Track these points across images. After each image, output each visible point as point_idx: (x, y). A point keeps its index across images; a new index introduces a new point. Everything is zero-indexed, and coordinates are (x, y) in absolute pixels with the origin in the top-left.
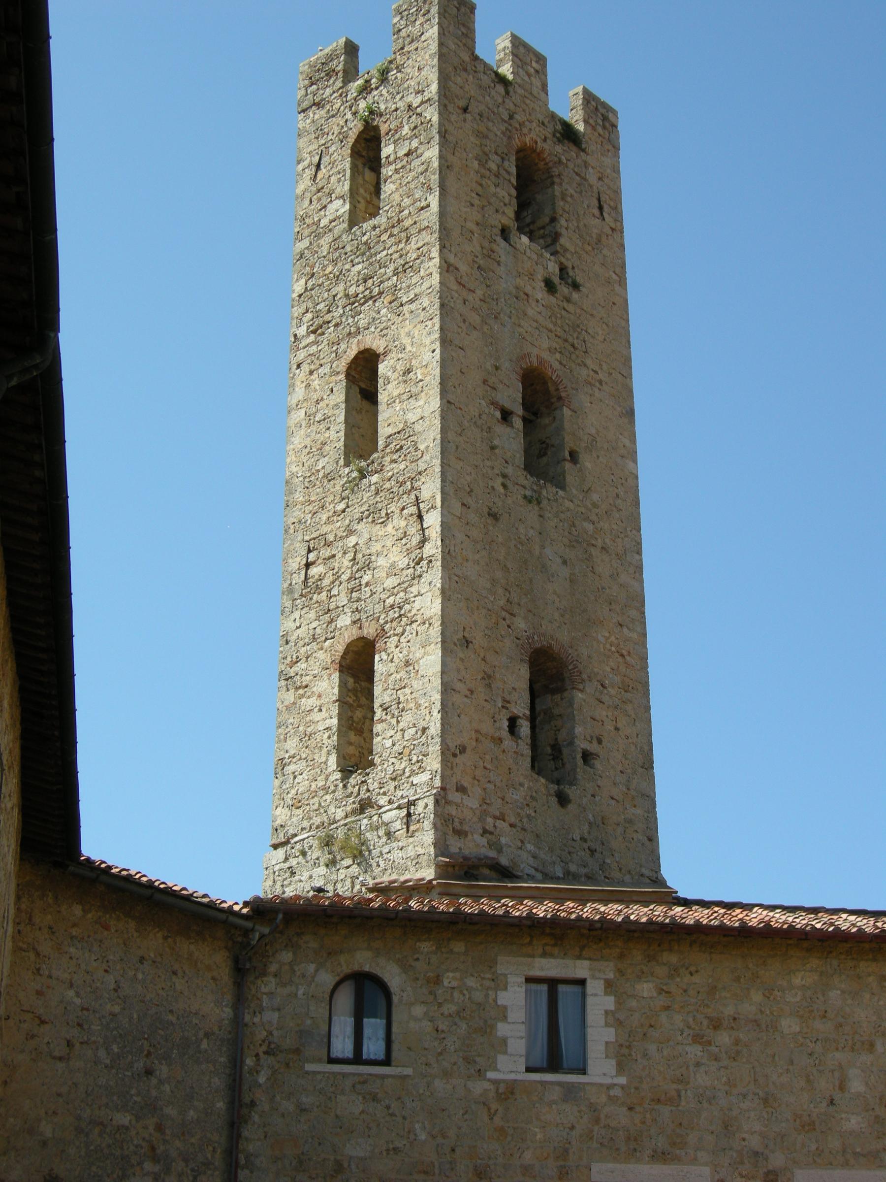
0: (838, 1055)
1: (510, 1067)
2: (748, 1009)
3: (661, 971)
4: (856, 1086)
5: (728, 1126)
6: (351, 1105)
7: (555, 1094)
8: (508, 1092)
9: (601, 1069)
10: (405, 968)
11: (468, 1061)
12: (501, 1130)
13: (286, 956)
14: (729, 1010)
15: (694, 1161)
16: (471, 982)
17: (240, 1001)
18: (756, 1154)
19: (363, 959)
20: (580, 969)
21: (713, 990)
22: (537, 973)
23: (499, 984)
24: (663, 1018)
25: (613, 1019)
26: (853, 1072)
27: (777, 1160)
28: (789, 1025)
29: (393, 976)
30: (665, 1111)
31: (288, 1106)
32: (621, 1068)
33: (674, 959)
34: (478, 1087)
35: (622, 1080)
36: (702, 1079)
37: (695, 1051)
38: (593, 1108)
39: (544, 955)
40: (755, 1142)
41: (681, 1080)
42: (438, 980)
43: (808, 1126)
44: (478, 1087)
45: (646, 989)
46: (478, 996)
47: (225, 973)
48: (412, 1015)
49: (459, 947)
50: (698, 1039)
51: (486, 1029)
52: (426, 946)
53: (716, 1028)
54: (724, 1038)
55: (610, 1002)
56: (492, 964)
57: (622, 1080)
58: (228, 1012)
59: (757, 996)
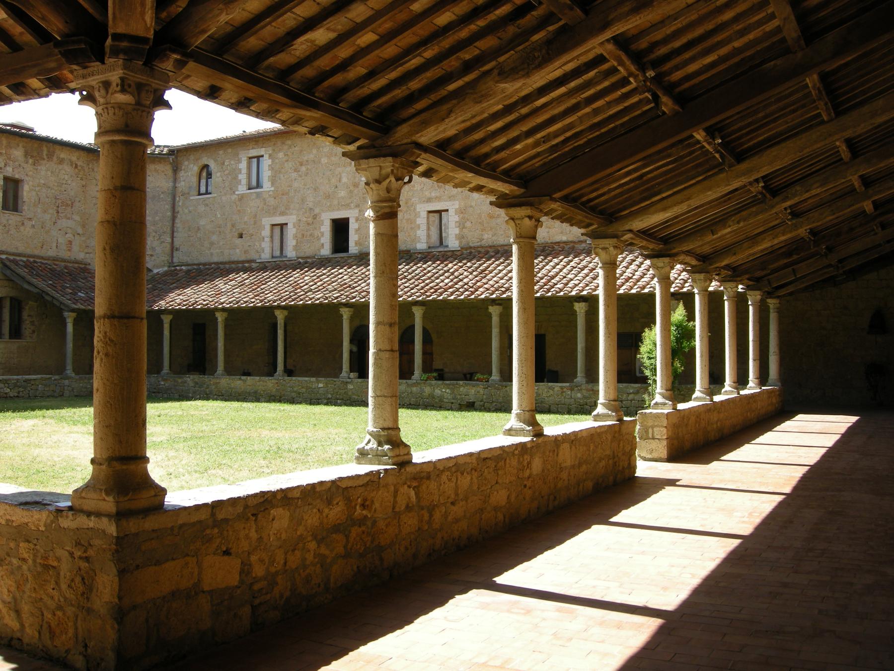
0: (339, 169)
1: (242, 189)
2: (311, 156)
3: (286, 147)
4: (344, 180)
5: (303, 200)
6: (202, 208)
7: (254, 196)
8: (242, 198)
9: (267, 186)
10: (215, 161)
11: (231, 189)
12: (239, 211)
13: (186, 163)
14: (306, 158)
15: (291, 214)
16: (232, 162)
17: (175, 180)
18: (311, 209)
19: (205, 161)
20: (261, 151)
21: (301, 151)
22: (250, 155)
23: (240, 161)
24: (286, 164)
25: (271, 168)
26: (343, 175)
27: (317, 211)
28: (324, 160)
29: (213, 166)
30: (285, 197)
31: (186, 211)
32: (273, 184)
33: (289, 142)
34: (234, 197)
35: (273, 189)
36: (296, 185)
37: (294, 175)
38: (264, 200)
39: (253, 148)
40: (311, 205)
41: (290, 186)
42: (223, 164)
43: (328, 197)
44: (234, 197)
45: (281, 155)
46: (234, 166)
47: (170, 173)
48: (217, 177)
49: (230, 150)
50: (296, 170)
51: (236, 178)
52: (221, 152)
53: (301, 165)
54: (303, 169)
55: (270, 162)
56: (238, 154)
57: (273, 189)
58: (171, 184)
59: (314, 151)
